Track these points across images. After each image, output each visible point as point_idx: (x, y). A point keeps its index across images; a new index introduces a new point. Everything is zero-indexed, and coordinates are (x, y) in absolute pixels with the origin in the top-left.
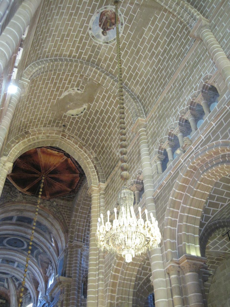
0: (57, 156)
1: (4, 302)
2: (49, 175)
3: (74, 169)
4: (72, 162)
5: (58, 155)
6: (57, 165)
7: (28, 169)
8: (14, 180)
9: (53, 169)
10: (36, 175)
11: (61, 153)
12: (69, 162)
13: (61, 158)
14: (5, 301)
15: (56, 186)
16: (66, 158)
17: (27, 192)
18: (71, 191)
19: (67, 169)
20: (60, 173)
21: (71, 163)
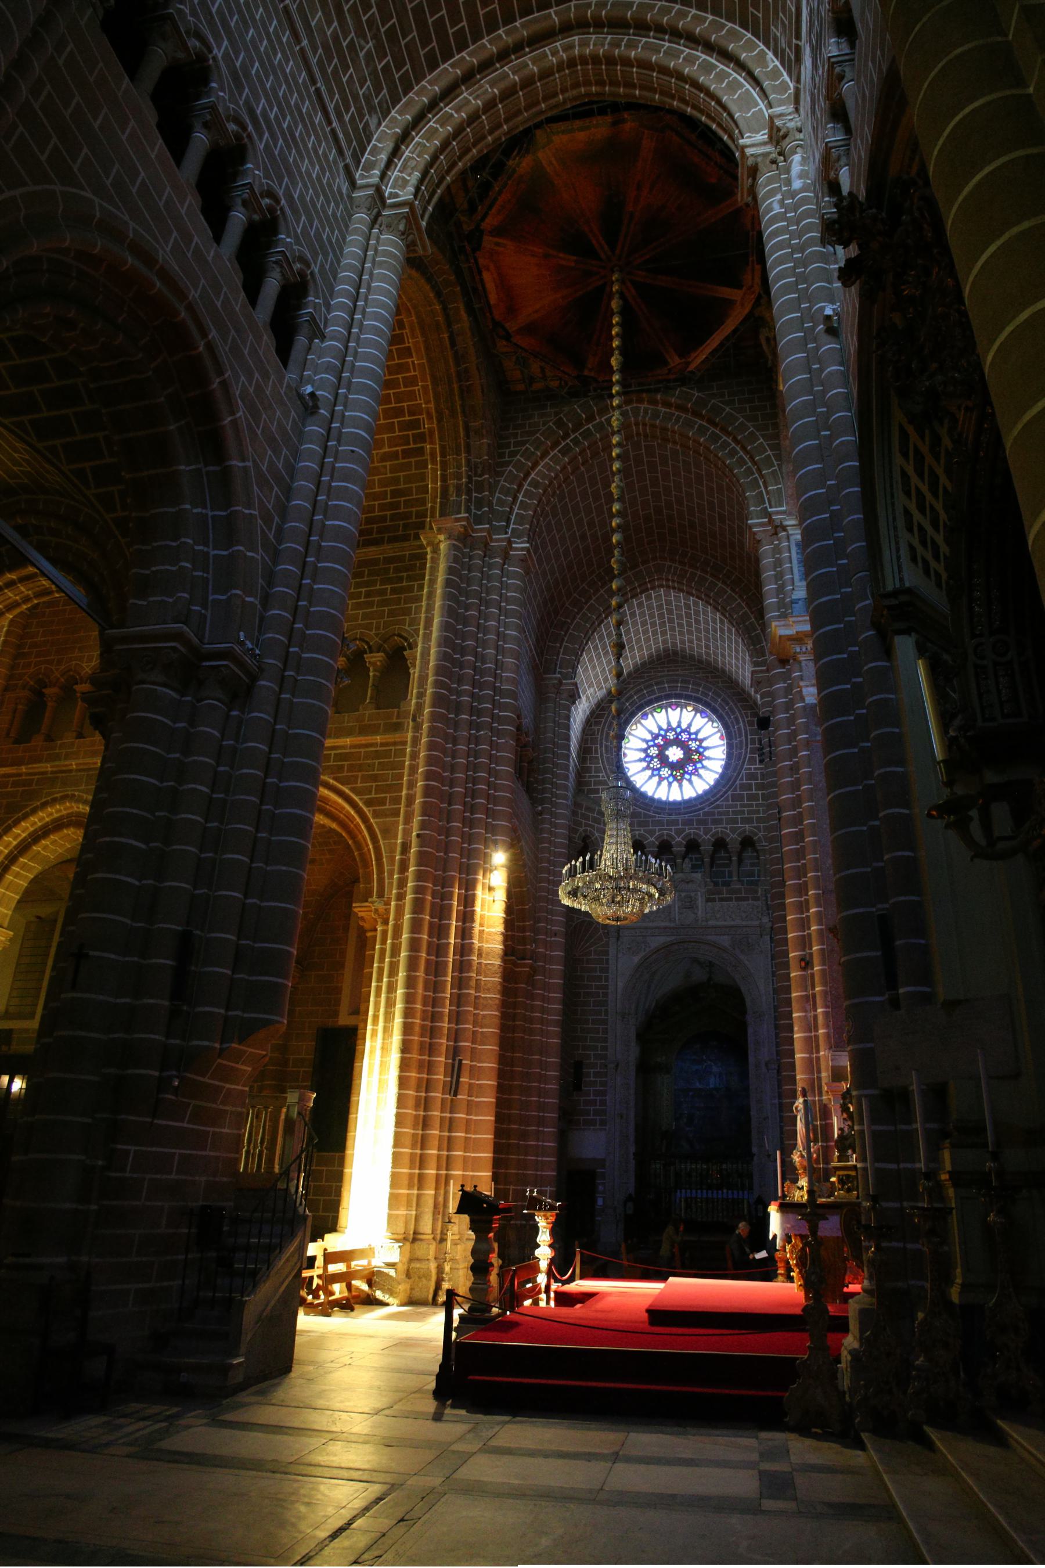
4: (494, 211)
6: (540, 251)
9: (561, 255)
11: (481, 261)
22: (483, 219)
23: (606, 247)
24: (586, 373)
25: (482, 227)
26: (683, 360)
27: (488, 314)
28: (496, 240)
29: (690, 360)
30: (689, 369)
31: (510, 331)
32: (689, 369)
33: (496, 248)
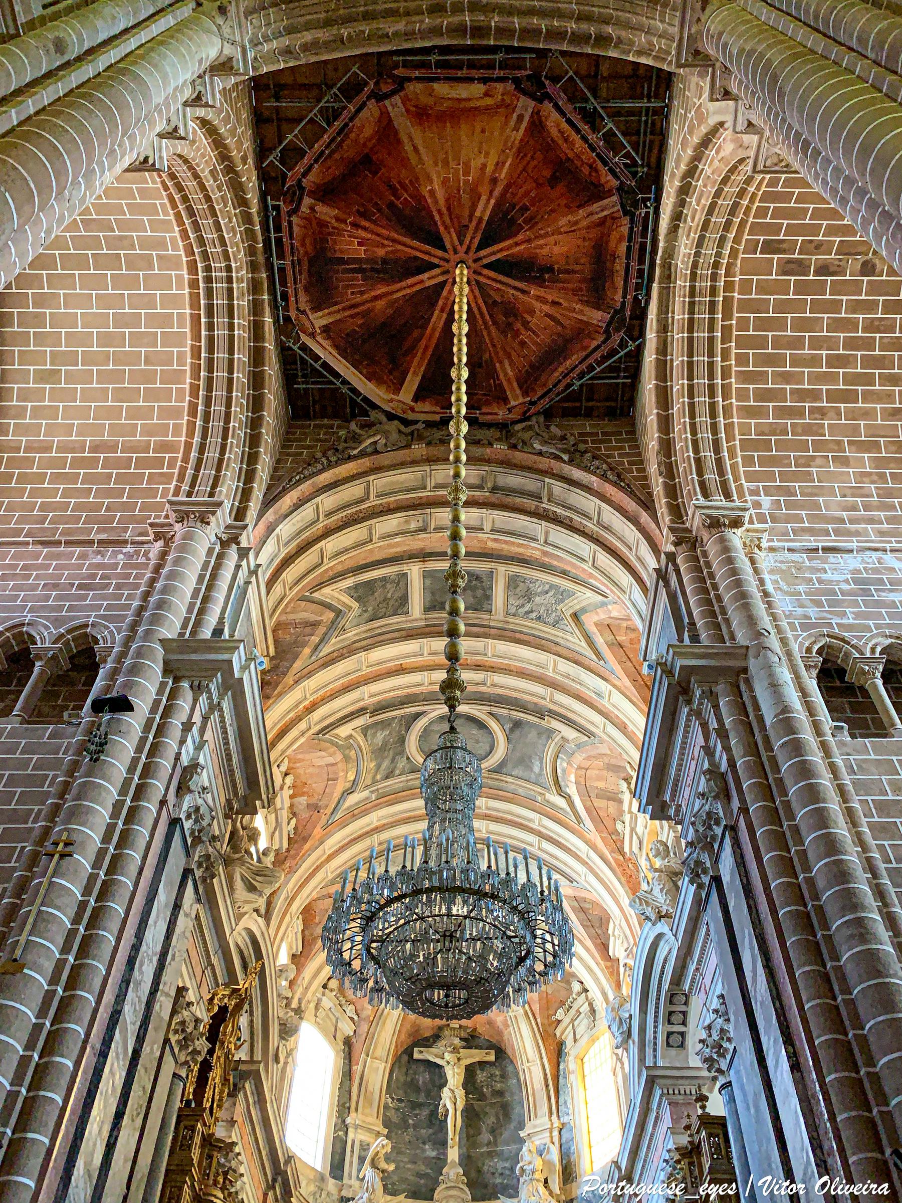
0: (487, 108)
1: (492, 1058)
2: (483, 253)
3: (586, 170)
4: (565, 126)
5: (489, 101)
6: (503, 176)
7: (381, 252)
8: (343, 353)
9: (493, 201)
10: (428, 279)
11: (500, 87)
12: (554, 132)
13: (507, 117)
14: (493, 1052)
15: (532, 312)
16: (530, 110)
17: (419, 406)
18: (609, 324)
19: (553, 181)
20: (531, 222)
21: (561, 132)
22: (557, 107)
23: (493, 258)
24: (307, 201)
25: (546, 102)
26: (318, 331)
27: (417, 74)
28: (526, 119)
29: (319, 338)
30: (302, 335)
31: (387, 102)
32: (302, 335)
33: (515, 115)
